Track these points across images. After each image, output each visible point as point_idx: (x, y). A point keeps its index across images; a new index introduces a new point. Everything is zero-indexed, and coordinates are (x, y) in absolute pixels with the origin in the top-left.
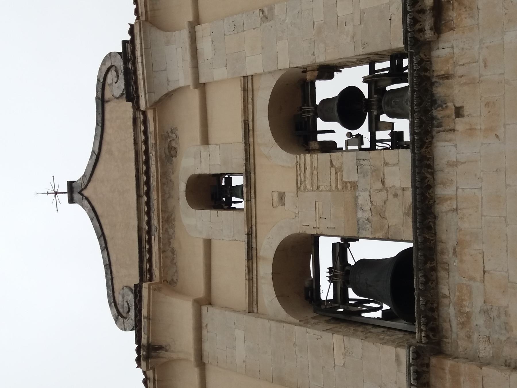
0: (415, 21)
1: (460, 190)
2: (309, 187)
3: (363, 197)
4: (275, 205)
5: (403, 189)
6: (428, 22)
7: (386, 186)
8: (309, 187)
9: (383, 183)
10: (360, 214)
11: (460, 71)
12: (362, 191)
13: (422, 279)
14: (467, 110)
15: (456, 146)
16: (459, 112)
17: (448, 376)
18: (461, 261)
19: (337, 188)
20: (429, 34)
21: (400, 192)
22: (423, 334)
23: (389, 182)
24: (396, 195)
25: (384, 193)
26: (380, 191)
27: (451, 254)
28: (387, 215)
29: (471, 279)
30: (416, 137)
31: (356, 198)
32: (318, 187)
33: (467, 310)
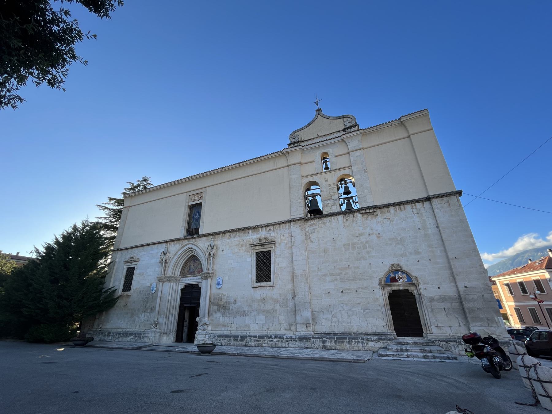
0: (364, 209)
2: (330, 187)
3: (329, 201)
4: (325, 179)
5: (332, 210)
6: (363, 212)
8: (330, 187)
9: (333, 206)
10: (326, 201)
11: (355, 219)
13: (316, 217)
14: (348, 221)
16: (347, 219)
21: (331, 209)
23: (333, 207)
24: (331, 209)
25: (331, 206)
26: (331, 205)
29: (318, 226)
31: (329, 200)
32: (330, 190)
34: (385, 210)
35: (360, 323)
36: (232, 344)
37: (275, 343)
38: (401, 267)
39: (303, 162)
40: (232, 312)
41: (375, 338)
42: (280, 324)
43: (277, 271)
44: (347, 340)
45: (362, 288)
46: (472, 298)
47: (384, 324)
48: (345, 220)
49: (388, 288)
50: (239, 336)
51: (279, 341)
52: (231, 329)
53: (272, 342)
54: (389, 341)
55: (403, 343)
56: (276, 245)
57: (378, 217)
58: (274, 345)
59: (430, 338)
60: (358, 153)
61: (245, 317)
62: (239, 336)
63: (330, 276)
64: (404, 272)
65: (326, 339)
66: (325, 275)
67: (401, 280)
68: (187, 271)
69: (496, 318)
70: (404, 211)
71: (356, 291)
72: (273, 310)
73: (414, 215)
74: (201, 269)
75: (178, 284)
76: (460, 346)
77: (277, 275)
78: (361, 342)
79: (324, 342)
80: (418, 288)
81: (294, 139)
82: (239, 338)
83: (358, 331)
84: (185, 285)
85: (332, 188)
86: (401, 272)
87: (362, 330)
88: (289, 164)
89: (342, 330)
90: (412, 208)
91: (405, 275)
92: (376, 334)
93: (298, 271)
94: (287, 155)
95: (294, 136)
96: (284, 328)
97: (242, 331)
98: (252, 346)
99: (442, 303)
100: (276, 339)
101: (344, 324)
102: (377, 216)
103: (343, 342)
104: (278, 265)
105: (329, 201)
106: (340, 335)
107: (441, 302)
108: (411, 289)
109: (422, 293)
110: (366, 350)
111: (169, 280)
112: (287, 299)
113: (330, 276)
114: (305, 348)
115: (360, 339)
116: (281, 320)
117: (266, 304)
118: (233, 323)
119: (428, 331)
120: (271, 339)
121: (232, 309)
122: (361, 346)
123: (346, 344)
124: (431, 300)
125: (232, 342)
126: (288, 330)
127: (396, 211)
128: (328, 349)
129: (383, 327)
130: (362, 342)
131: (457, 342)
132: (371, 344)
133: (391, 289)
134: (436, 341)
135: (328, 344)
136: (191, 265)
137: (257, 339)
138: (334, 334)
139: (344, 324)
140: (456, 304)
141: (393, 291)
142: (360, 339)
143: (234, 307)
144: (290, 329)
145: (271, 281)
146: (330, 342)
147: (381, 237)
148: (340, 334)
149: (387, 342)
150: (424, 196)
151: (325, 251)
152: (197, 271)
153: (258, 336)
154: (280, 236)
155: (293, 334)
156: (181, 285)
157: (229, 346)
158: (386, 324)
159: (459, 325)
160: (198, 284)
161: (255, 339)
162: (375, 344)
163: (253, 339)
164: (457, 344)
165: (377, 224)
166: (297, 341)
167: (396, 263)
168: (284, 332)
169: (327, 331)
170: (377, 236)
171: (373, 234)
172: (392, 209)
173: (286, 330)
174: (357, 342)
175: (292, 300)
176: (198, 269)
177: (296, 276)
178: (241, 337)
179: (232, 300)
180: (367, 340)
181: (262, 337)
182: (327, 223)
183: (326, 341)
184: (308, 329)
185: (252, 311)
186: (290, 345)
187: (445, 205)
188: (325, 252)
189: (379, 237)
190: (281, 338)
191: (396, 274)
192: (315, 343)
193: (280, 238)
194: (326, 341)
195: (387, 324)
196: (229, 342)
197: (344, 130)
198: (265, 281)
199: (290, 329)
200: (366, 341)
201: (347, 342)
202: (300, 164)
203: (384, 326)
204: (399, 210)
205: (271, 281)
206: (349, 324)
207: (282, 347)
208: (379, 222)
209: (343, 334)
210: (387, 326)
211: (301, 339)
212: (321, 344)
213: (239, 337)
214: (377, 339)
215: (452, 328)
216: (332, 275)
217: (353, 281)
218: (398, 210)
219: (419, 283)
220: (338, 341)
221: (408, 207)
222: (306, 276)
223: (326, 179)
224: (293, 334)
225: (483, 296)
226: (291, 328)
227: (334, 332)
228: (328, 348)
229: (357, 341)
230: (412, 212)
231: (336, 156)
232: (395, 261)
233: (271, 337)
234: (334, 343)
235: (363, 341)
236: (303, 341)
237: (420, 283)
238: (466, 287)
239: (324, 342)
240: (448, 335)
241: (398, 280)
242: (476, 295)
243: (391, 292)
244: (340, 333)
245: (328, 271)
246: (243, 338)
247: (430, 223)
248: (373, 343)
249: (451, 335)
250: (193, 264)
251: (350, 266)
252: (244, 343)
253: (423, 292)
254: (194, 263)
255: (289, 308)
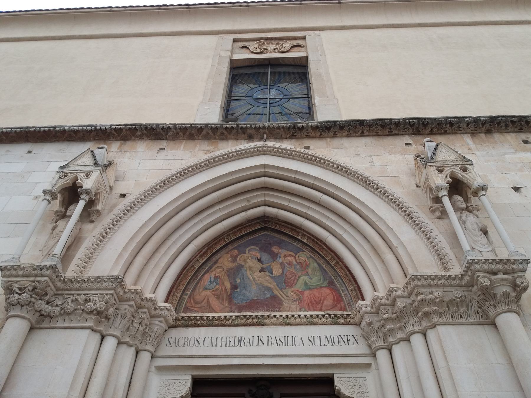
68: (218, 297)
74: (327, 291)
75: (145, 357)
84: (197, 382)
111: (101, 305)
136: (241, 267)
152: (300, 301)
156: (171, 378)
160: (329, 381)
176: (300, 285)
250: (260, 261)
254: (265, 257)
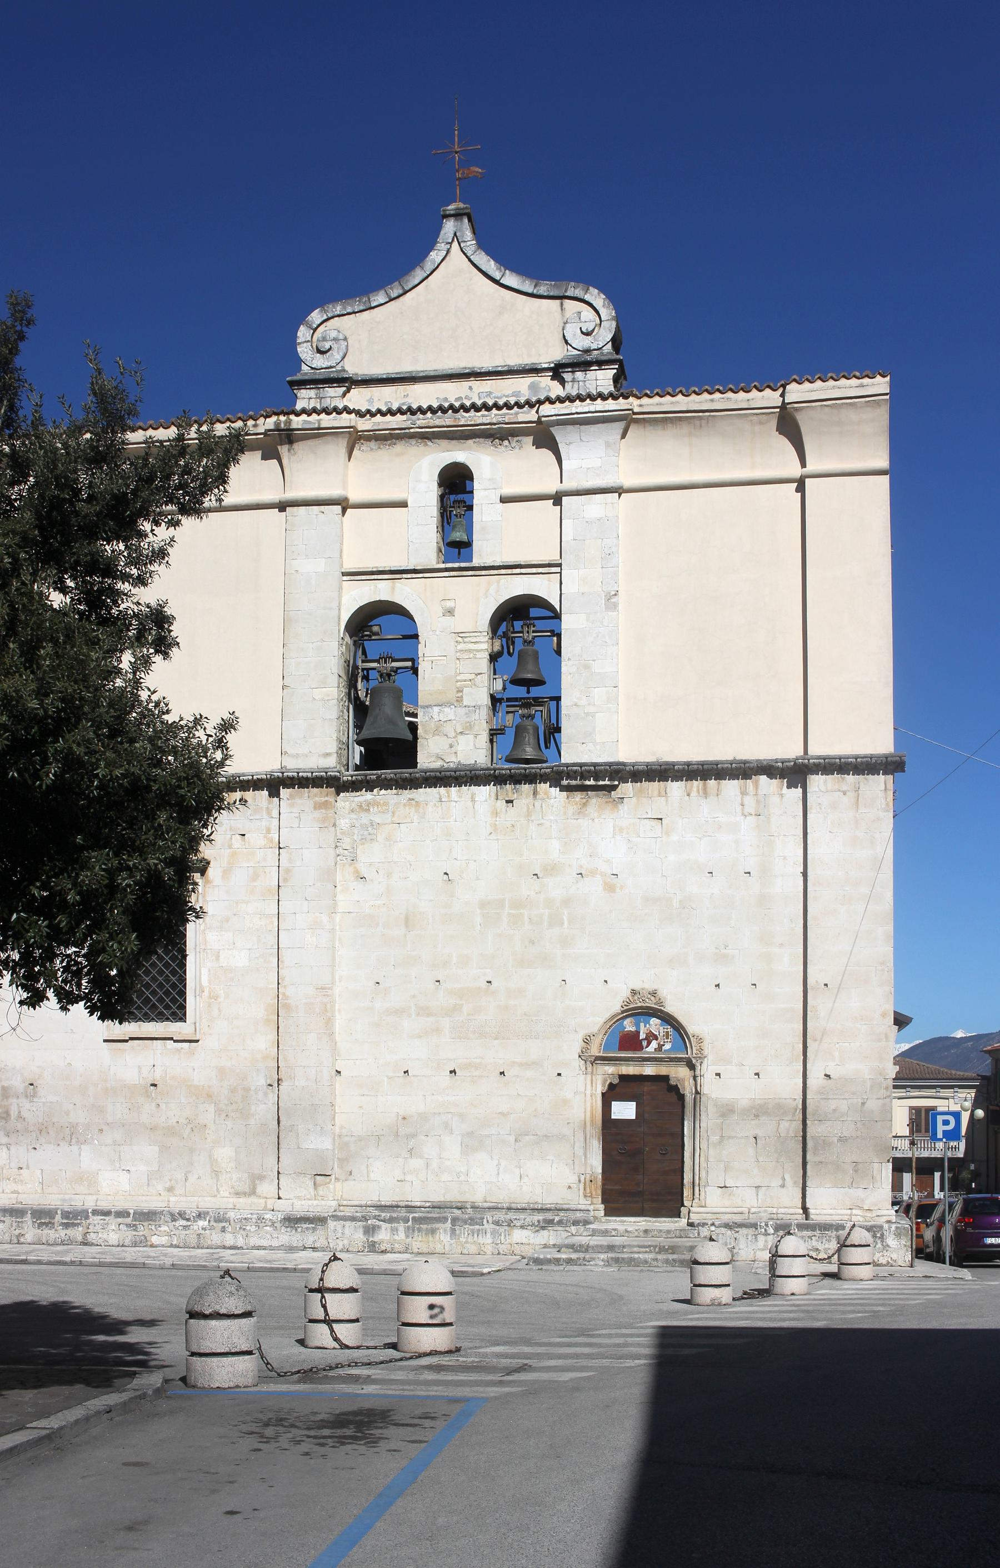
1: (454, 803)
2: (459, 647)
3: (449, 713)
7: (459, 736)
8: (459, 647)
10: (436, 709)
12: (455, 712)
15: (486, 801)
17: (323, 799)
18: (405, 805)
19: (457, 682)
20: (565, 782)
21: (453, 750)
22: (350, 778)
23: (461, 739)
24: (451, 746)
25: (453, 734)
26: (455, 731)
27: (409, 796)
28: (437, 737)
30: (492, 772)
31: (449, 704)
33: (371, 809)
34: (654, 787)
35: (498, 1174)
36: (29, 1237)
37: (199, 1235)
38: (660, 1003)
39: (354, 497)
40: (19, 1126)
41: (540, 1217)
42: (216, 1173)
43: (210, 982)
44: (448, 1225)
45: (521, 1065)
46: (834, 1110)
47: (573, 1179)
48: (501, 804)
49: (607, 1068)
50: (59, 1212)
51: (212, 1228)
52: (20, 1188)
53: (187, 1232)
54: (573, 1228)
55: (614, 1233)
56: (210, 871)
57: (625, 808)
58: (193, 1240)
59: (695, 1218)
60: (595, 506)
61: (75, 1148)
62: (59, 1212)
63: (418, 1015)
64: (668, 1019)
65: (378, 1223)
66: (400, 1012)
67: (654, 1044)
69: (876, 1166)
70: (716, 798)
71: (502, 1073)
72: (190, 1126)
73: (743, 817)
76: (761, 1239)
77: (210, 997)
78: (488, 1231)
79: (370, 1230)
80: (698, 1073)
81: (319, 351)
82: (58, 1218)
83: (487, 1200)
85: (470, 651)
86: (658, 1017)
87: (502, 1197)
88: (291, 495)
89: (438, 1196)
90: (744, 793)
91: (670, 1029)
92: (542, 1209)
93: (296, 992)
94: (283, 450)
95: (324, 339)
96: (233, 1187)
97: (67, 1197)
98: (111, 1244)
99: (753, 1122)
100: (202, 1223)
101: (445, 1177)
102: (620, 807)
103: (433, 1232)
104: (218, 958)
105: (447, 710)
106: (428, 1212)
107: (752, 1117)
108: (679, 1073)
109: (705, 1090)
110: (501, 1252)
112: (247, 1090)
113: (418, 1015)
114: (305, 1248)
115: (488, 1221)
116: (219, 1160)
117: (163, 1106)
118: (24, 1167)
119: (696, 1200)
120: (184, 1223)
121: (20, 1117)
122: (490, 1241)
123: (442, 1238)
124: (727, 1111)
125: (30, 1232)
126: (245, 1194)
127: (688, 795)
128: (382, 1252)
129: (570, 1187)
130: (494, 1233)
131: (756, 1229)
132: (519, 1235)
133: (616, 1073)
134: (704, 1225)
135: (383, 1235)
137: (129, 1220)
138: (407, 1207)
139: (445, 1177)
140: (791, 1126)
141: (623, 1078)
142: (488, 1221)
143: (30, 1111)
144: (253, 1192)
145: (182, 1018)
146: (389, 1230)
147: (618, 890)
148: (429, 1207)
149: (567, 1229)
150: (790, 750)
151: (407, 919)
153: (132, 1212)
154: (229, 836)
155: (266, 1206)
157: (18, 1243)
158: (580, 1181)
159: (781, 1182)
161: (120, 1220)
162: (532, 1235)
163: (113, 1222)
164: (756, 1233)
165: (614, 834)
166: (278, 1228)
167: (650, 986)
168: (231, 1200)
169: (386, 1199)
170: (606, 884)
171: (593, 872)
172: (676, 788)
173: (237, 1194)
174: (479, 1230)
175: (266, 1094)
177: (288, 1007)
178: (66, 1215)
179: (17, 1084)
180: (509, 1225)
181: (148, 1216)
182: (430, 808)
183: (379, 1227)
184: (321, 1193)
185: (105, 1128)
186: (254, 1241)
187: (845, 799)
188: (407, 926)
189: (610, 888)
190: (220, 1219)
191: (642, 1025)
192: (339, 1235)
193: (230, 847)
194: (379, 1227)
195: (582, 1178)
196: (17, 1232)
197: (557, 371)
198: (161, 1017)
199: (253, 1192)
200: (506, 1228)
201: (445, 1230)
202: (338, 509)
203: (571, 1185)
204: (698, 791)
205: (182, 1018)
206: (462, 1178)
207: (224, 1247)
208: (621, 830)
209: (436, 1207)
210: (582, 1186)
211: (292, 1221)
212: (359, 1236)
213: (56, 1213)
214: (539, 1221)
215: (762, 1191)
216: (424, 1011)
217: (496, 1039)
218: (694, 793)
219: (701, 1058)
220: (418, 1229)
221: (731, 787)
222: (326, 1011)
223: (449, 604)
224: (266, 1206)
225: (863, 1104)
226: (259, 1190)
227: (410, 1204)
228: (383, 1248)
229: (477, 1227)
230: (739, 809)
231: (504, 500)
232: (644, 982)
233: (182, 1215)
234: (401, 1235)
235: (498, 1228)
236: (299, 1230)
237: (705, 1057)
238: (828, 1076)
239: (370, 1230)
240: (746, 1210)
241: (645, 1043)
242: (845, 1102)
243: (616, 1081)
244: (428, 1204)
245: (414, 996)
246: (73, 1217)
247: (785, 858)
248: (525, 1233)
249: (753, 1210)
251: (494, 984)
252: (77, 1233)
253: (710, 1087)
255: (252, 1122)
